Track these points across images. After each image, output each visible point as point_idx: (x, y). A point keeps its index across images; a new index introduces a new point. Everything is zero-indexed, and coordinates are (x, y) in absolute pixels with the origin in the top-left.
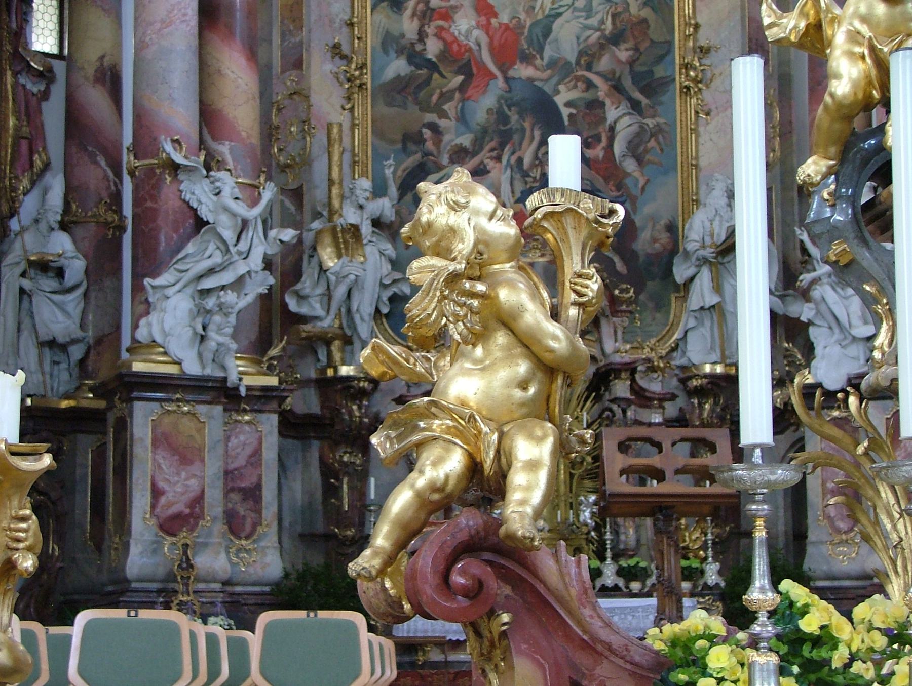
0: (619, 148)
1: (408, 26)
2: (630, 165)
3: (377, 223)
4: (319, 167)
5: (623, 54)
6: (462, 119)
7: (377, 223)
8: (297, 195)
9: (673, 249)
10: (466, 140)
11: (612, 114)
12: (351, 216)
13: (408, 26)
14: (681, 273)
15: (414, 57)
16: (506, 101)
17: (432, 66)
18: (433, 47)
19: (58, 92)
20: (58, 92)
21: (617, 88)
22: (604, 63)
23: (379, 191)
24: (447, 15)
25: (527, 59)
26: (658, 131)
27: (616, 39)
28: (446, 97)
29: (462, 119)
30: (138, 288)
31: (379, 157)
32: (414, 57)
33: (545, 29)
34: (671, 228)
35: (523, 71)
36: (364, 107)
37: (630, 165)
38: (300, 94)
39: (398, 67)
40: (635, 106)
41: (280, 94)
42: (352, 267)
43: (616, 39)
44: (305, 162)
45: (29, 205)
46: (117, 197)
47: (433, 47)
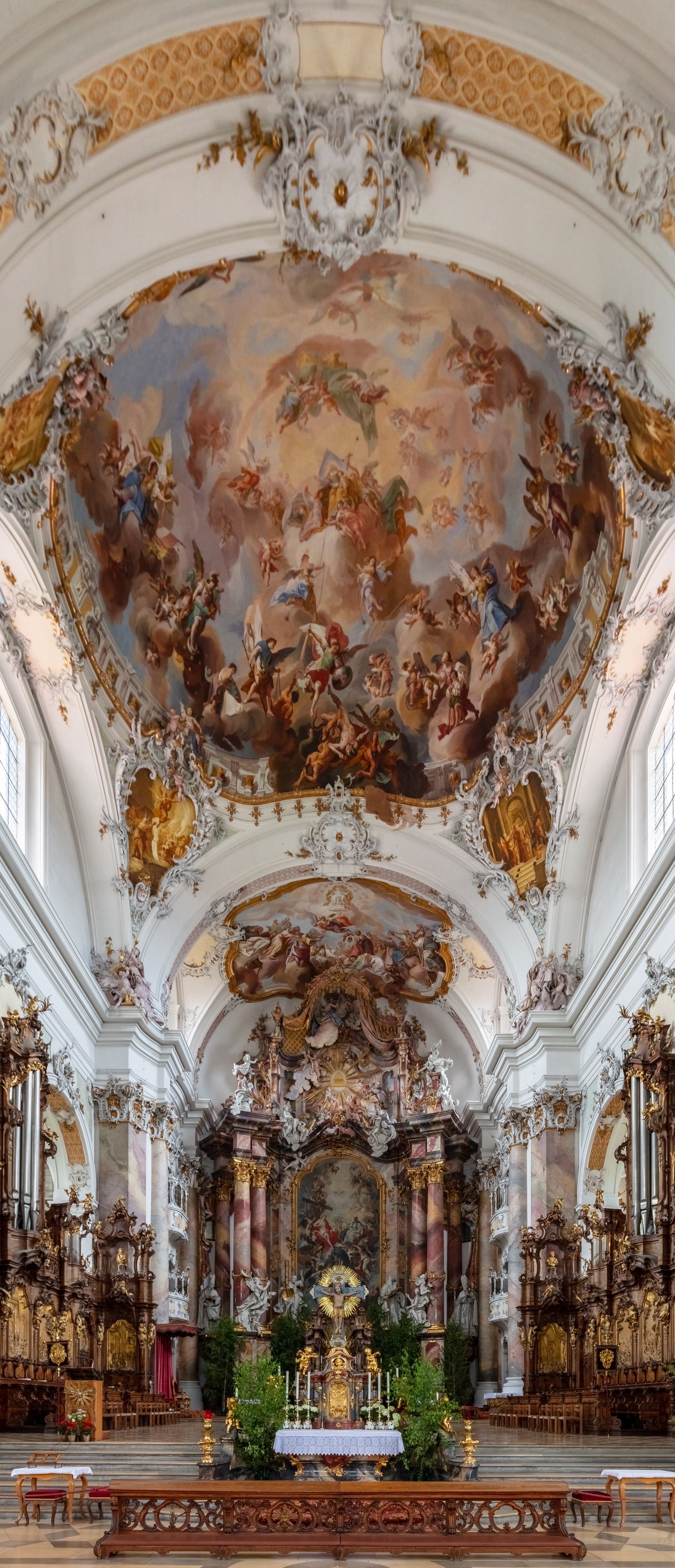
0: (364, 1267)
1: (307, 1232)
2: (367, 1272)
3: (298, 1287)
4: (283, 1272)
5: (366, 1241)
6: (322, 1258)
7: (298, 1287)
8: (277, 1279)
9: (378, 1295)
10: (323, 1264)
11: (362, 1257)
12: (291, 1286)
13: (307, 1232)
14: (379, 1302)
15: (309, 1240)
16: (334, 1253)
17: (314, 1243)
18: (314, 1238)
19: (213, 1249)
20: (213, 1249)
21: (364, 1250)
22: (361, 1243)
23: (299, 1278)
24: (318, 1229)
25: (340, 1242)
26: (375, 1262)
27: (363, 1236)
28: (317, 1252)
29: (322, 1258)
30: (235, 1309)
31: (299, 1269)
32: (309, 1240)
33: (344, 1233)
34: (378, 1289)
35: (339, 1245)
36: (295, 1255)
37: (367, 1272)
38: (278, 1251)
39: (304, 1243)
40: (369, 1255)
41: (272, 1251)
42: (291, 1301)
43: (363, 1236)
44: (280, 1270)
45: (205, 1281)
46: (229, 1280)
47: (314, 1238)
